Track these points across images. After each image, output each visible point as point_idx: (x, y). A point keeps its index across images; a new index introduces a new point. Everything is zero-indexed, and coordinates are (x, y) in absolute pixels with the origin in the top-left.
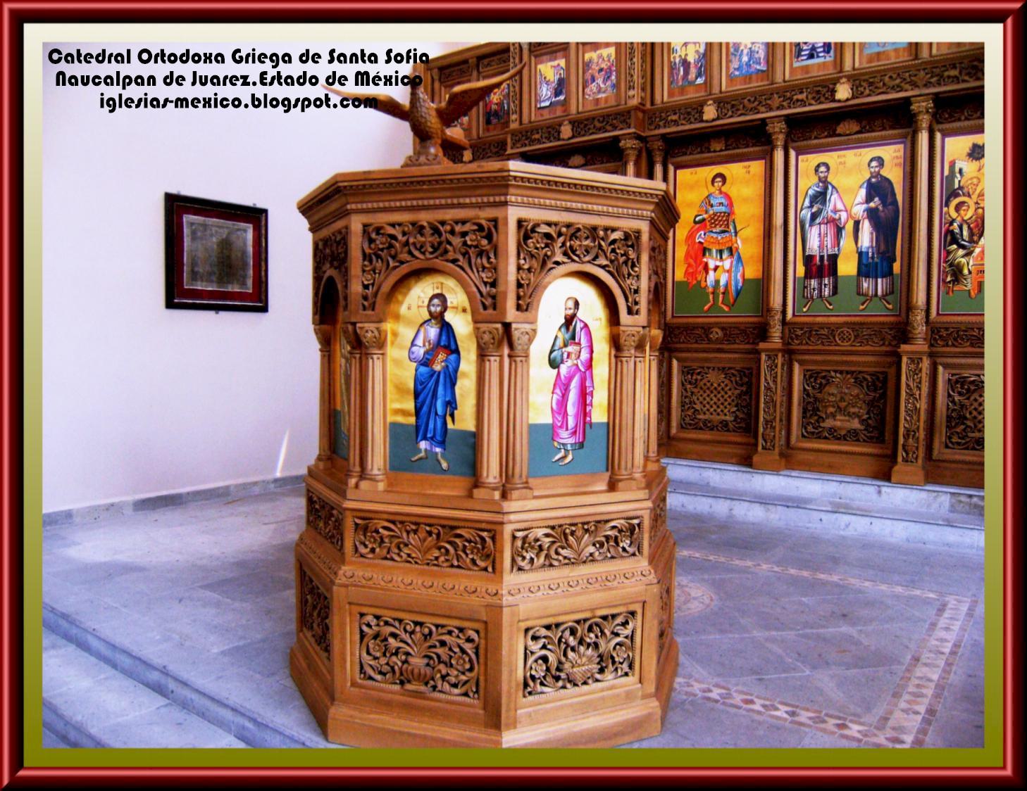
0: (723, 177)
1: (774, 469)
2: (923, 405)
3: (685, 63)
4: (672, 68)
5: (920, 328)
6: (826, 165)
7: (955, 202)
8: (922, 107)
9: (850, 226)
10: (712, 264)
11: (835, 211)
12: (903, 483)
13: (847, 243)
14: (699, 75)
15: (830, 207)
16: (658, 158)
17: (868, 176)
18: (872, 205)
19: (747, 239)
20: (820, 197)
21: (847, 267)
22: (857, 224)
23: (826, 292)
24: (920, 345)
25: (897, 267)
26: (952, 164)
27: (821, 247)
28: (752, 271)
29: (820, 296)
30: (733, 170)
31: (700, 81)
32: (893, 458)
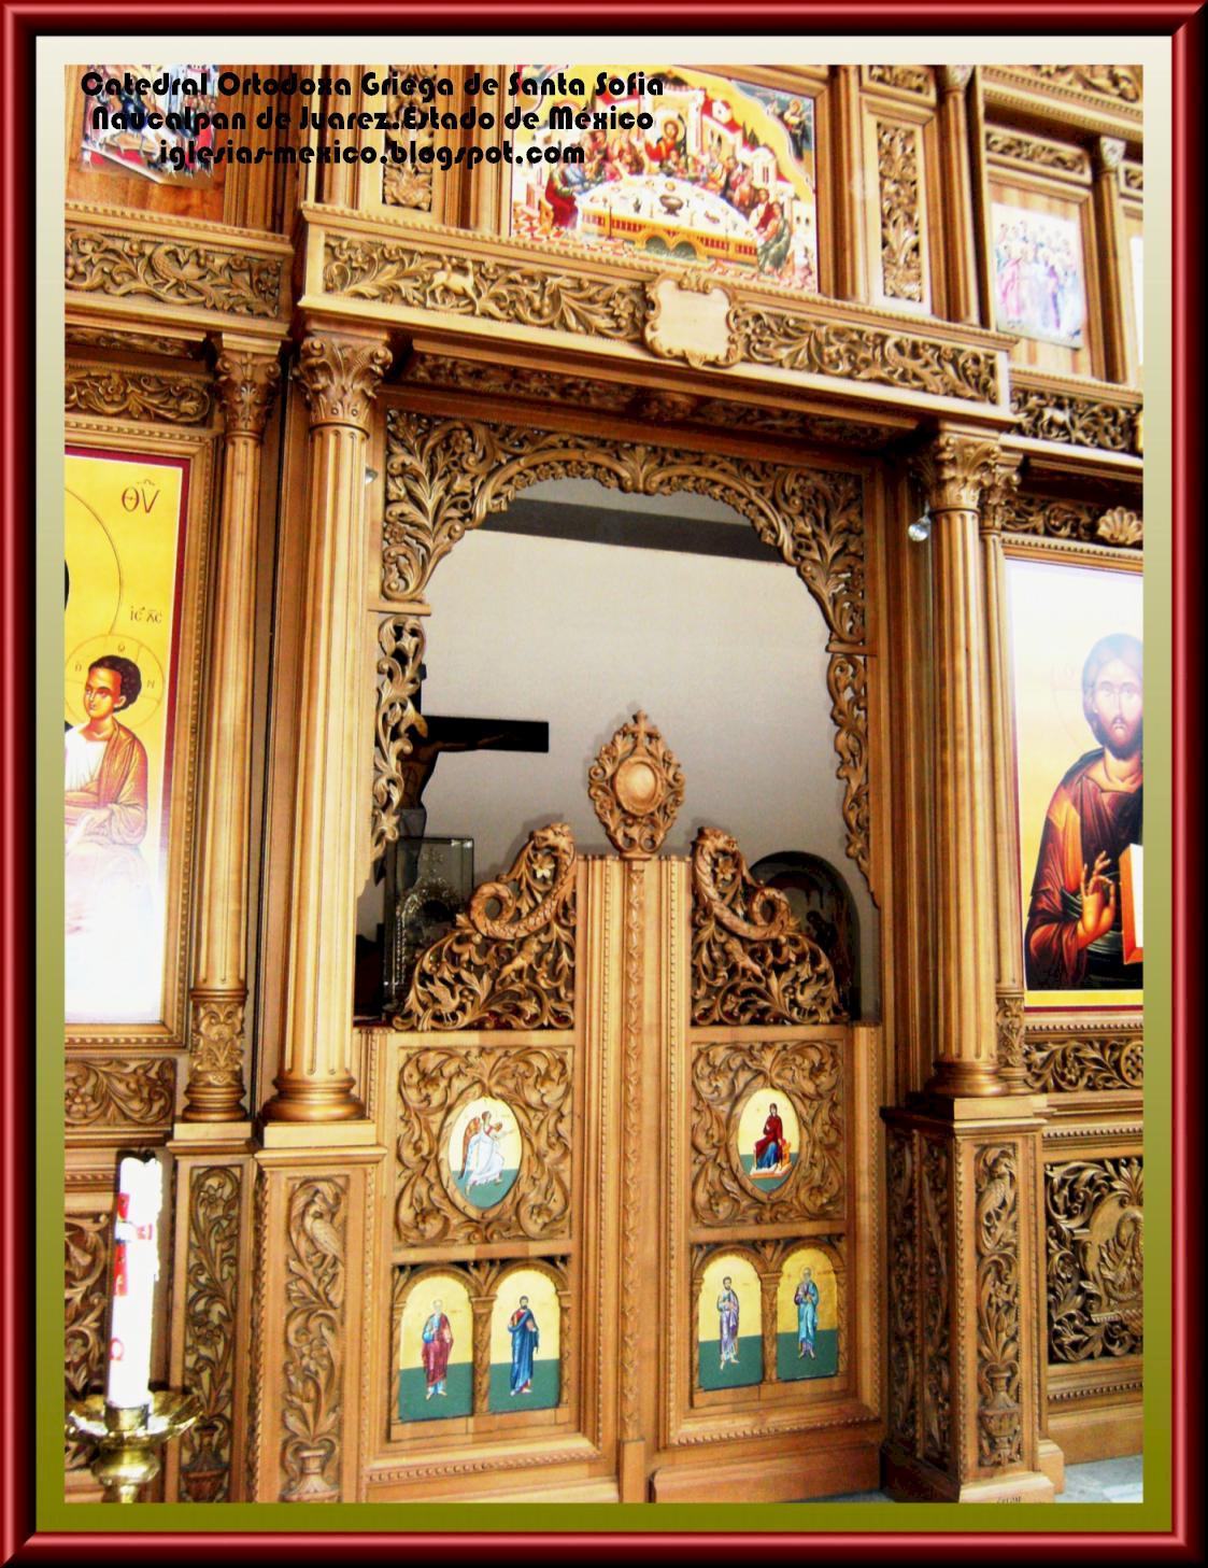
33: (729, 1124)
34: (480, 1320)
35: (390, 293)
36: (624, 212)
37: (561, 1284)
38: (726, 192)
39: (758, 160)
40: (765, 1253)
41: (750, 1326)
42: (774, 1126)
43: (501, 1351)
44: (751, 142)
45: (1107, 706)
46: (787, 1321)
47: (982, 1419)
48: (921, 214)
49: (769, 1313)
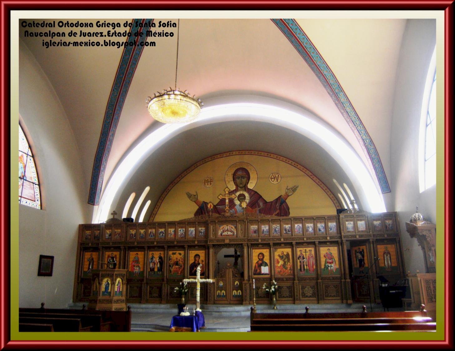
0: (137, 254)
1: (144, 303)
2: (166, 291)
3: (132, 234)
4: (130, 235)
5: (165, 279)
6: (153, 253)
7: (170, 260)
8: (166, 247)
9: (156, 263)
10: (135, 269)
11: (154, 261)
12: (163, 304)
13: (156, 266)
14: (135, 237)
15: (154, 260)
16: (127, 250)
17: (159, 256)
18: (159, 260)
19: (141, 265)
20: (152, 259)
21: (156, 270)
22: (157, 263)
23: (153, 274)
24: (165, 282)
25: (163, 270)
26: (170, 255)
27: (152, 266)
28: (142, 270)
29: (152, 274)
30: (139, 253)
31: (134, 238)
32: (162, 300)
33: (234, 283)
34: (221, 292)
35: (212, 243)
36: (225, 234)
37: (225, 291)
38: (231, 232)
39: (232, 229)
40: (237, 290)
41: (236, 294)
42: (237, 283)
43: (222, 294)
44: (232, 228)
45: (260, 257)
46: (238, 294)
47: (245, 299)
48: (243, 230)
49: (237, 293)
